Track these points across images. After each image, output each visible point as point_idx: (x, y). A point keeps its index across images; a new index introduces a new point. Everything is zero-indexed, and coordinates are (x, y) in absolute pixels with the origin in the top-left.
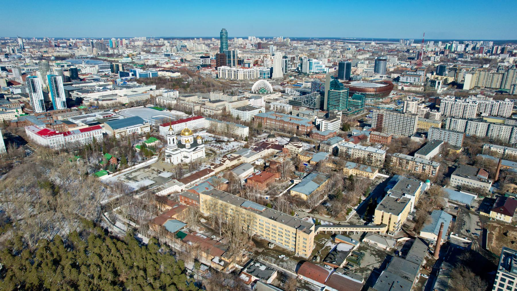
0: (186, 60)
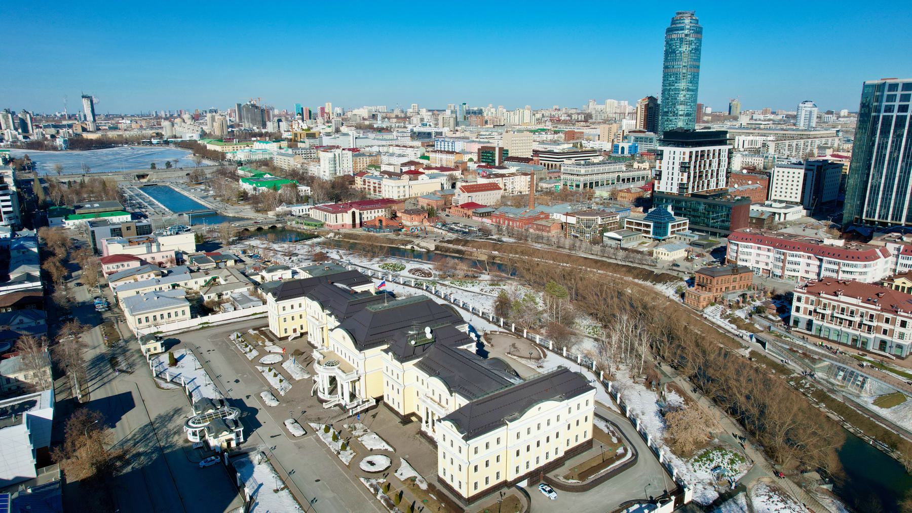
0: (503, 152)
